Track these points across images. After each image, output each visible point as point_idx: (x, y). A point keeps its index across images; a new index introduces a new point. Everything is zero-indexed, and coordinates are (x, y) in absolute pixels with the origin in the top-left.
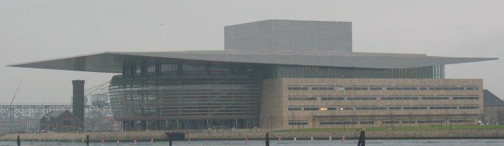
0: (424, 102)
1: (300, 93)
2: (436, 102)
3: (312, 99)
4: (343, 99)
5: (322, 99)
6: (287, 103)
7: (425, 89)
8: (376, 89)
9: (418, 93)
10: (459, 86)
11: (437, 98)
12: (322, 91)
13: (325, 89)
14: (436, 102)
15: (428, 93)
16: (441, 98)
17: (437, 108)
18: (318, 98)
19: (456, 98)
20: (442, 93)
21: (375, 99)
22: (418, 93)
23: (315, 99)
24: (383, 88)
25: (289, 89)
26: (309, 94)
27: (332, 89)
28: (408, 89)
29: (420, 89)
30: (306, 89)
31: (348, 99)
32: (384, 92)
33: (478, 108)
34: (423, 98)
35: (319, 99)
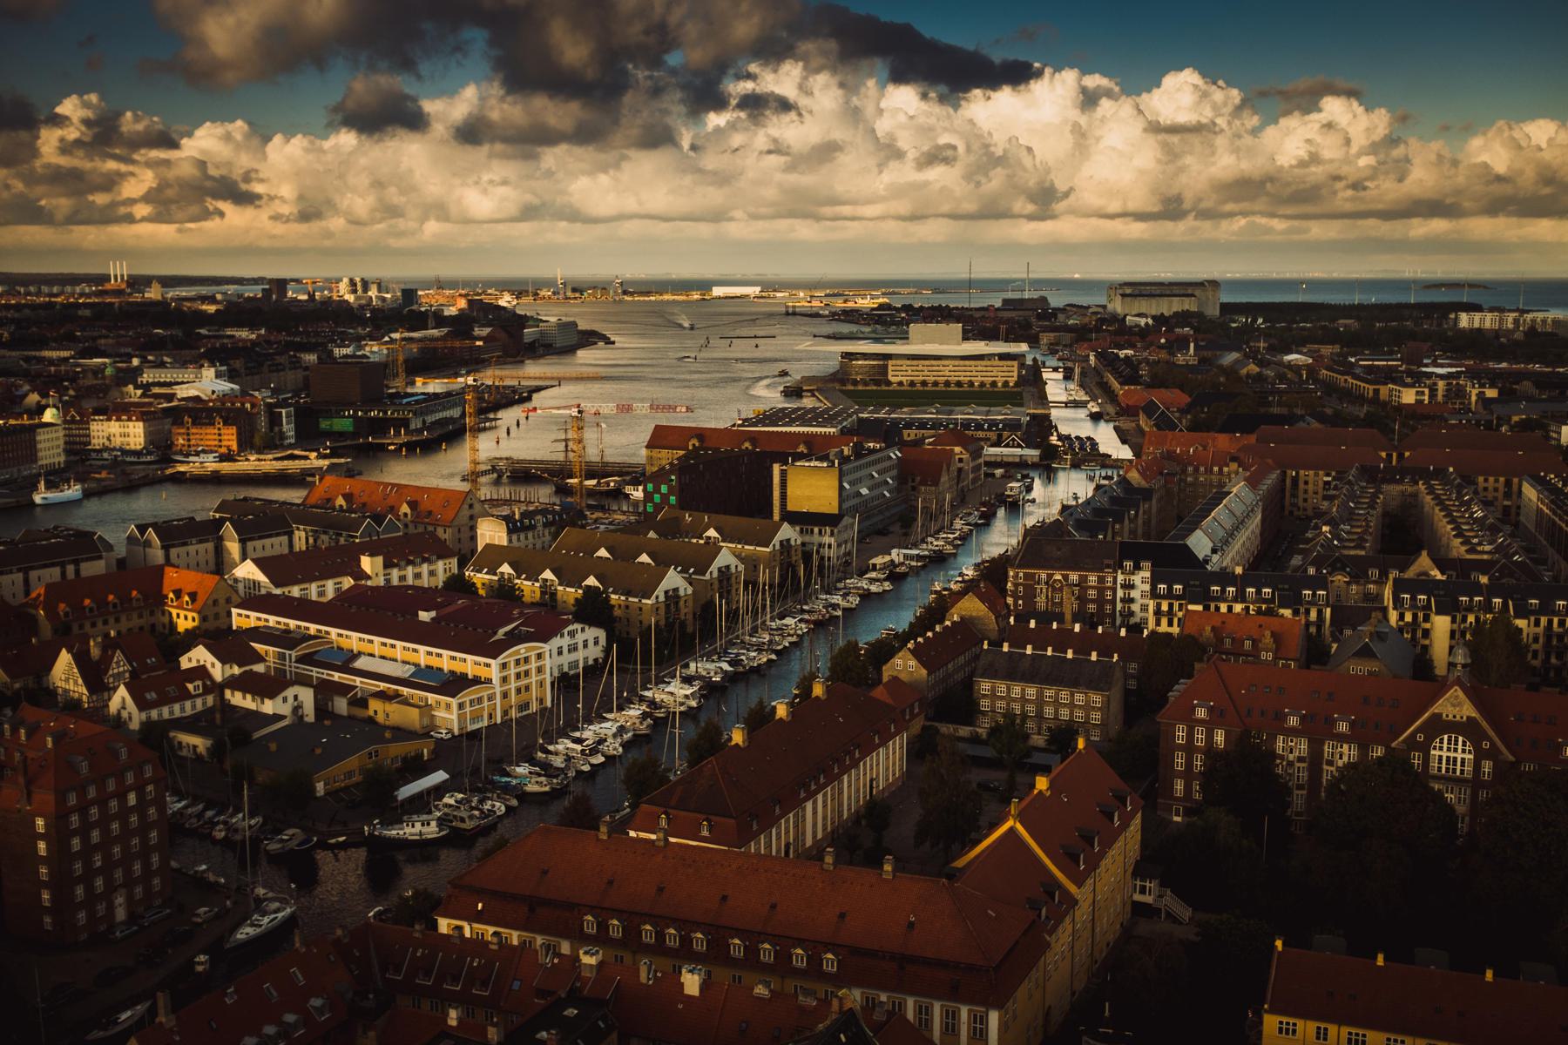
1: (899, 368)
2: (984, 374)
14: (984, 374)
15: (980, 368)
20: (989, 368)
26: (904, 368)
32: (951, 368)
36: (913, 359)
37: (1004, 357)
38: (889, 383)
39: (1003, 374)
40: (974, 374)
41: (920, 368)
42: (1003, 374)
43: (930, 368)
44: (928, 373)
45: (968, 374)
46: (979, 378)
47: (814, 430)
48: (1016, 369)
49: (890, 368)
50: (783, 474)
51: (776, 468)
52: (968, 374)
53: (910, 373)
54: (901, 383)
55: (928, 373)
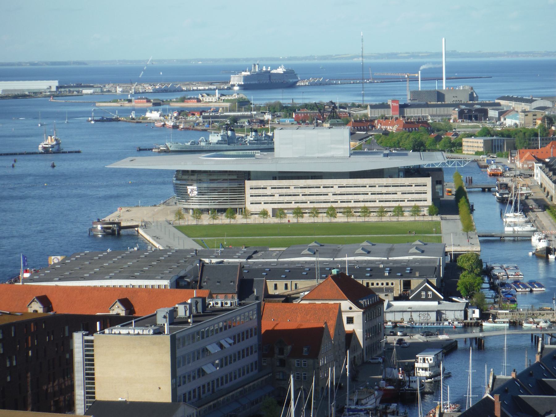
0: (374, 197)
3: (271, 196)
4: (299, 195)
5: (280, 195)
6: (248, 199)
7: (375, 186)
8: (329, 187)
9: (367, 189)
10: (407, 184)
11: (386, 194)
12: (280, 189)
13: (283, 188)
15: (377, 190)
16: (390, 194)
17: (385, 201)
18: (276, 195)
19: (405, 193)
21: (327, 195)
22: (367, 189)
23: (274, 196)
24: (335, 186)
25: (251, 188)
26: (269, 191)
27: (289, 188)
28: (359, 187)
29: (370, 186)
30: (266, 188)
31: (303, 195)
32: (337, 190)
33: (426, 200)
34: (372, 194)
35: (277, 195)
36: (275, 178)
37: (410, 172)
38: (244, 212)
39: (410, 197)
40: (370, 197)
41: (292, 191)
42: (410, 197)
43: (307, 191)
44: (304, 198)
45: (361, 198)
46: (378, 204)
47: (136, 283)
48: (429, 189)
49: (248, 192)
50: (89, 345)
51: (78, 339)
52: (361, 198)
53: (277, 198)
54: (264, 213)
55: (304, 198)
